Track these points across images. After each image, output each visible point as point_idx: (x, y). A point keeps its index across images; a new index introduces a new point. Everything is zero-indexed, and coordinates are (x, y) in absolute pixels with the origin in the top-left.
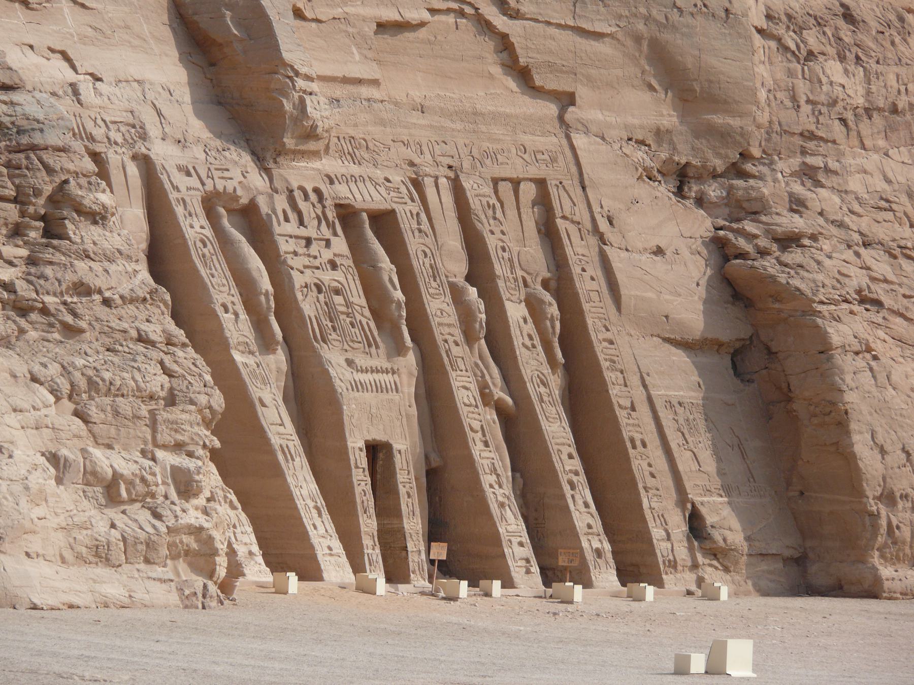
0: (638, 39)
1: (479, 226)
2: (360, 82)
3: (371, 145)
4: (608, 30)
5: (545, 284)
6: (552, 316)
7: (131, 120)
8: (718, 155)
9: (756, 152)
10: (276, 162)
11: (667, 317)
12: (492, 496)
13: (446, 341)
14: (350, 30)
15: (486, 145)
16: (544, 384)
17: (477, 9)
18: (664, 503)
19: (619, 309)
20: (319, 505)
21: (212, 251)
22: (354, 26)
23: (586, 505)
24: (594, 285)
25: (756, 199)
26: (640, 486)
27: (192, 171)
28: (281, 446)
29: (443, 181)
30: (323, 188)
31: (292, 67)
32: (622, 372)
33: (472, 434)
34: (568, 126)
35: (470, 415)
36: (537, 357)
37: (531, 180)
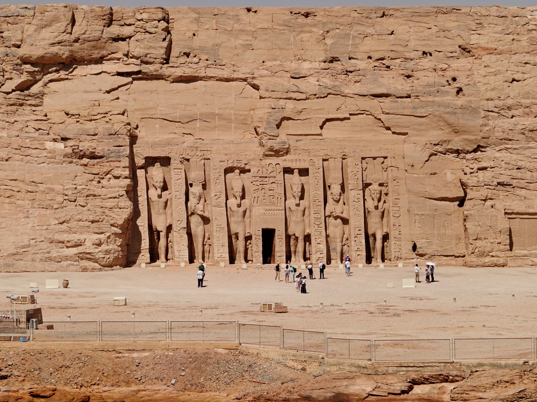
2: (312, 135)
8: (470, 147)
15: (362, 149)
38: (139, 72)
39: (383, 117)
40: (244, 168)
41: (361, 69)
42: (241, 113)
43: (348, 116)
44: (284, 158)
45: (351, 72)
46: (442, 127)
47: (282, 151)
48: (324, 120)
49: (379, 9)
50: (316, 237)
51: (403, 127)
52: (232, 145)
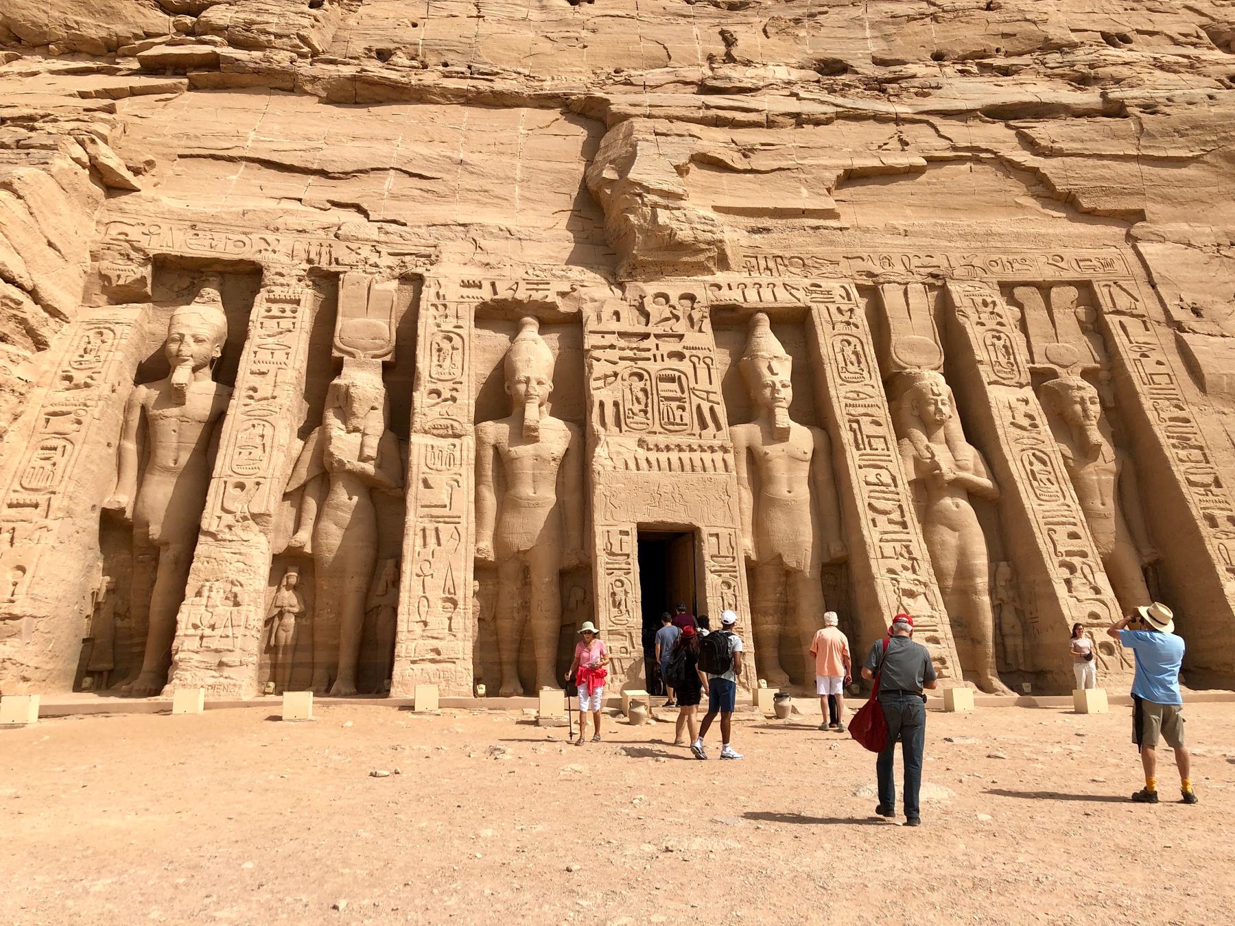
1: (962, 319)
2: (804, 213)
4: (1190, 155)
5: (1086, 374)
6: (1082, 398)
10: (630, 275)
12: (888, 582)
13: (858, 422)
14: (802, 176)
15: (994, 257)
16: (1044, 463)
17: (995, 153)
21: (460, 347)
23: (1097, 591)
24: (1161, 369)
27: (487, 286)
28: (424, 530)
29: (916, 289)
30: (700, 294)
31: (640, 185)
32: (1201, 448)
33: (871, 515)
34: (1136, 239)
37: (1069, 283)
38: (212, 62)
39: (1046, 165)
40: (553, 306)
42: (544, 165)
44: (709, 278)
45: (890, 81)
47: (703, 250)
48: (841, 172)
50: (896, 564)
51: (1123, 193)
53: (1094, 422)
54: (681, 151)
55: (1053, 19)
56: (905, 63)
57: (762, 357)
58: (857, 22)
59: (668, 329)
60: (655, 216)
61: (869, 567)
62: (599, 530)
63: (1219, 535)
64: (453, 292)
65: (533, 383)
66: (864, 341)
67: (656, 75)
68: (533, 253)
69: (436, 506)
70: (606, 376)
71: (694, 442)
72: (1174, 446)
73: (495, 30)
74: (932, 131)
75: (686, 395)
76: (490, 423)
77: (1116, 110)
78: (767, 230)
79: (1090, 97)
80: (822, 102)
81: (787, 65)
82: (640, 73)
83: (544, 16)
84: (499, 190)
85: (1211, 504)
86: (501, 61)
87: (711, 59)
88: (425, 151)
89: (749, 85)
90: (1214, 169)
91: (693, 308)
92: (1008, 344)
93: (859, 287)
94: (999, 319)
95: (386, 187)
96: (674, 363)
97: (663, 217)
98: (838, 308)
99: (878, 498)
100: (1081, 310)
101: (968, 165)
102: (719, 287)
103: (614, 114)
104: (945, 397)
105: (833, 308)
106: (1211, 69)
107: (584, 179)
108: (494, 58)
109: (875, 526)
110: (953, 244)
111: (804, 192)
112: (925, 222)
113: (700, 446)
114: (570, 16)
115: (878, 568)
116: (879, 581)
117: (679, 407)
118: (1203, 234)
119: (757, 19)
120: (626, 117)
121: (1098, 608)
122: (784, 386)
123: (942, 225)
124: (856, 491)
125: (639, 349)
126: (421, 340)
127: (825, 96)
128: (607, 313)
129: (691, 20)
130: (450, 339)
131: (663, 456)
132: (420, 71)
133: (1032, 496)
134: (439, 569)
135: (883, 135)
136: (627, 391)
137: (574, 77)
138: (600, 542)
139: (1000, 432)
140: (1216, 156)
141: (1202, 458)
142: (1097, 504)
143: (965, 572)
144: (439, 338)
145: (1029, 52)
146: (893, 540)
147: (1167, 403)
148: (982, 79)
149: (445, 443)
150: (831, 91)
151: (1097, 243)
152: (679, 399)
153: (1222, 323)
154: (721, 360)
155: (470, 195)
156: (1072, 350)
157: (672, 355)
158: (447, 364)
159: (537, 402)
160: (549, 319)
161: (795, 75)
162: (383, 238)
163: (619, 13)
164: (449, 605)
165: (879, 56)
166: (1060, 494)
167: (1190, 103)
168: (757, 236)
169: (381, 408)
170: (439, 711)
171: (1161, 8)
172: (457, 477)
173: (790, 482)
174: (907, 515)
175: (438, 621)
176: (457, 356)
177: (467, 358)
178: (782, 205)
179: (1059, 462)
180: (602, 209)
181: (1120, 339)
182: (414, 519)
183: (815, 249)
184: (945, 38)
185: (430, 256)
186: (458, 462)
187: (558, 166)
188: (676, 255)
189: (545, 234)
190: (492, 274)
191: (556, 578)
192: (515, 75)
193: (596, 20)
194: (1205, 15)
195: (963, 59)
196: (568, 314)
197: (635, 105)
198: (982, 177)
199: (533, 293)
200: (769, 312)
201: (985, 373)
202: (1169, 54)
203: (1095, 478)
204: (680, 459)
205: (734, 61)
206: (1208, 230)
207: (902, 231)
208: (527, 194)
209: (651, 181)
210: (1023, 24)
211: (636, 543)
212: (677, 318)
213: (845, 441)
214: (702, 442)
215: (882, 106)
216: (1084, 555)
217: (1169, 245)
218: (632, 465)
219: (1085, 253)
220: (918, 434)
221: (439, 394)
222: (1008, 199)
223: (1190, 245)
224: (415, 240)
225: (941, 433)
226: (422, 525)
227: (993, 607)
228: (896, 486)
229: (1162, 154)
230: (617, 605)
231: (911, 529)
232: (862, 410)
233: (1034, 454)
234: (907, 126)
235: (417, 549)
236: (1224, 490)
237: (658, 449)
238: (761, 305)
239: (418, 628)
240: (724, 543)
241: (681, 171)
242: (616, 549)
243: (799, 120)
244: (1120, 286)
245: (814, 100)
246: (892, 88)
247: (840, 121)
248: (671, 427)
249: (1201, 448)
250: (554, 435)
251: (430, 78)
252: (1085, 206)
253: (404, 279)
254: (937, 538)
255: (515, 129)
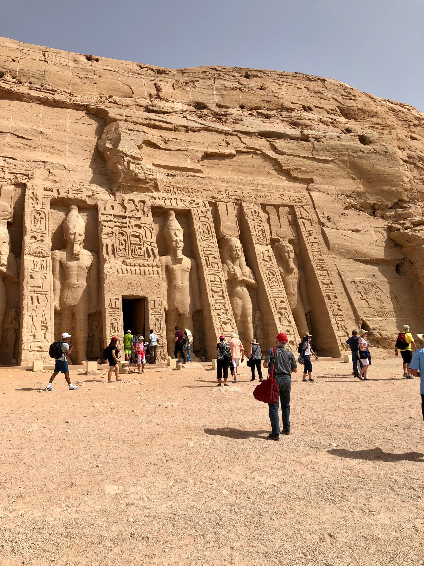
0: (344, 162)
1: (247, 218)
2: (188, 170)
3: (190, 190)
4: (330, 159)
5: (290, 241)
6: (288, 250)
7: (28, 173)
9: (406, 199)
10: (118, 190)
11: (356, 251)
12: (217, 319)
13: (208, 257)
14: (188, 154)
15: (260, 194)
16: (274, 275)
17: (262, 151)
18: (346, 321)
19: (329, 248)
20: (48, 325)
22: (191, 153)
23: (290, 322)
24: (316, 241)
25: (406, 213)
26: (331, 314)
27: (55, 190)
28: (32, 297)
30: (147, 200)
31: (123, 152)
32: (327, 270)
33: (212, 293)
34: (310, 190)
35: (213, 285)
36: (272, 265)
40: (85, 201)
41: (234, 114)
42: (79, 137)
43: (234, 152)
44: (150, 194)
46: (353, 176)
47: (148, 182)
48: (203, 154)
49: (241, 69)
50: (220, 312)
52: (65, 171)
53: (292, 260)
54: (140, 139)
55: (285, 97)
56: (229, 108)
57: (172, 229)
58: (210, 87)
59: (134, 215)
60: (129, 166)
61: (211, 313)
62: (106, 298)
63: (331, 302)
64: (40, 193)
65: (77, 235)
66: (211, 224)
67: (127, 101)
68: (75, 177)
69: (36, 287)
70: (108, 234)
71: (146, 263)
72: (318, 269)
73: (54, 69)
74: (239, 140)
75: (142, 243)
76: (57, 251)
77: (305, 138)
78: (174, 176)
79: (296, 132)
80: (197, 122)
81: (182, 103)
82: (120, 99)
83: (76, 65)
84: (59, 147)
85: (329, 291)
86: (57, 85)
87: (150, 96)
88: (25, 126)
89: (167, 111)
90: (338, 165)
91: (144, 207)
92: (263, 229)
93: (209, 202)
94: (260, 219)
95: (6, 141)
96: (137, 229)
97: (132, 167)
98: (201, 211)
99: (215, 287)
100: (290, 216)
101: (252, 155)
102: (155, 199)
103: (110, 118)
104: (239, 248)
105: (199, 211)
106: (339, 125)
107: (97, 145)
108: (53, 83)
109: (213, 297)
110: (244, 187)
111: (189, 161)
112: (235, 177)
113: (148, 265)
114: (88, 67)
115: (214, 313)
116: (214, 318)
117: (139, 248)
118: (332, 190)
119: (170, 80)
120: (116, 120)
121: (289, 328)
122: (180, 241)
123: (241, 179)
124: (207, 284)
125: (122, 223)
126: (26, 213)
127: (197, 119)
128: (108, 206)
129: (142, 76)
130: (40, 214)
131: (133, 268)
132: (19, 85)
133: (269, 287)
134: (39, 313)
135: (220, 139)
136: (118, 240)
137: (91, 97)
138: (107, 303)
139: (259, 262)
140: (338, 160)
141: (327, 274)
142: (291, 290)
143: (244, 315)
144: (34, 213)
145: (276, 110)
146: (219, 303)
147: (317, 253)
148: (257, 119)
149: (39, 260)
150: (200, 117)
151: (296, 190)
152: (139, 245)
153: (337, 224)
154: (156, 228)
155: (46, 148)
156: (286, 231)
157: (136, 226)
158: (39, 224)
159: (79, 243)
160: (83, 207)
161: (185, 108)
162: (6, 165)
163: (111, 69)
164: (44, 328)
165: (219, 103)
166: (278, 287)
167: (331, 139)
168: (170, 178)
169: (8, 242)
170: (44, 371)
171: (324, 98)
172: (45, 274)
173: (182, 279)
174: (225, 293)
175: (40, 335)
176: (43, 221)
177: (47, 222)
178: (180, 166)
179: (279, 274)
180: (105, 160)
181: (302, 228)
182: (27, 293)
183: (193, 185)
184: (245, 99)
185: (28, 175)
186: (45, 268)
187: (85, 138)
188: (137, 184)
189: (80, 169)
190: (57, 185)
191: (86, 317)
192: (64, 93)
193: (100, 71)
194: (338, 102)
195: (251, 109)
196: (91, 205)
197: (119, 115)
198: (256, 160)
199: (76, 195)
200: (174, 210)
201: (255, 240)
202: (326, 117)
203: (291, 280)
204: (140, 269)
205: (160, 98)
206: (334, 189)
207: (226, 181)
208: (72, 150)
209: (127, 151)
210: (274, 97)
211: (122, 304)
212: (138, 211)
213: (203, 264)
214: (148, 263)
215: (220, 126)
216: (286, 309)
217: (321, 193)
218: (120, 271)
219: (292, 194)
220: (229, 262)
221: (35, 238)
222: (266, 170)
223: (328, 194)
224: (21, 167)
225: (237, 262)
226: (31, 295)
227: (254, 328)
228: (221, 282)
229: (320, 158)
230: (114, 328)
231: (226, 299)
232: (209, 252)
233: (270, 271)
234: (229, 136)
235: (29, 305)
236: (334, 286)
237: (131, 265)
238: (171, 207)
239: (31, 338)
240: (157, 304)
241: (139, 147)
242: (113, 306)
243: (187, 129)
244: (303, 208)
245: (193, 120)
246: (224, 118)
247: (204, 131)
248: (136, 256)
249: (327, 270)
250: (86, 258)
251: (24, 89)
252: (293, 175)
253: (17, 185)
254: (235, 302)
255: (65, 119)
